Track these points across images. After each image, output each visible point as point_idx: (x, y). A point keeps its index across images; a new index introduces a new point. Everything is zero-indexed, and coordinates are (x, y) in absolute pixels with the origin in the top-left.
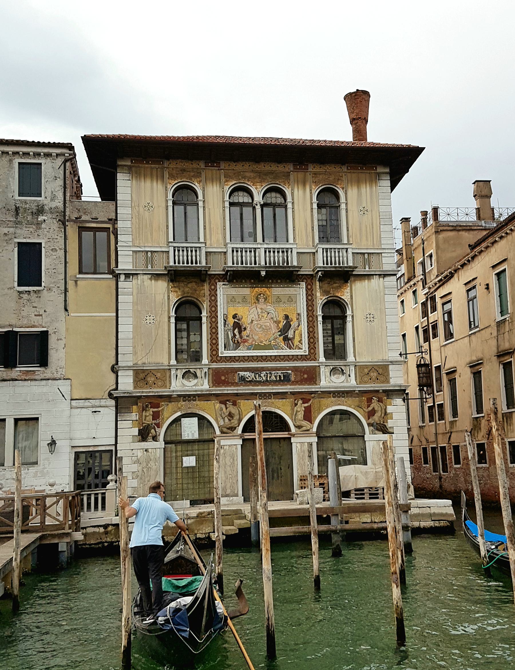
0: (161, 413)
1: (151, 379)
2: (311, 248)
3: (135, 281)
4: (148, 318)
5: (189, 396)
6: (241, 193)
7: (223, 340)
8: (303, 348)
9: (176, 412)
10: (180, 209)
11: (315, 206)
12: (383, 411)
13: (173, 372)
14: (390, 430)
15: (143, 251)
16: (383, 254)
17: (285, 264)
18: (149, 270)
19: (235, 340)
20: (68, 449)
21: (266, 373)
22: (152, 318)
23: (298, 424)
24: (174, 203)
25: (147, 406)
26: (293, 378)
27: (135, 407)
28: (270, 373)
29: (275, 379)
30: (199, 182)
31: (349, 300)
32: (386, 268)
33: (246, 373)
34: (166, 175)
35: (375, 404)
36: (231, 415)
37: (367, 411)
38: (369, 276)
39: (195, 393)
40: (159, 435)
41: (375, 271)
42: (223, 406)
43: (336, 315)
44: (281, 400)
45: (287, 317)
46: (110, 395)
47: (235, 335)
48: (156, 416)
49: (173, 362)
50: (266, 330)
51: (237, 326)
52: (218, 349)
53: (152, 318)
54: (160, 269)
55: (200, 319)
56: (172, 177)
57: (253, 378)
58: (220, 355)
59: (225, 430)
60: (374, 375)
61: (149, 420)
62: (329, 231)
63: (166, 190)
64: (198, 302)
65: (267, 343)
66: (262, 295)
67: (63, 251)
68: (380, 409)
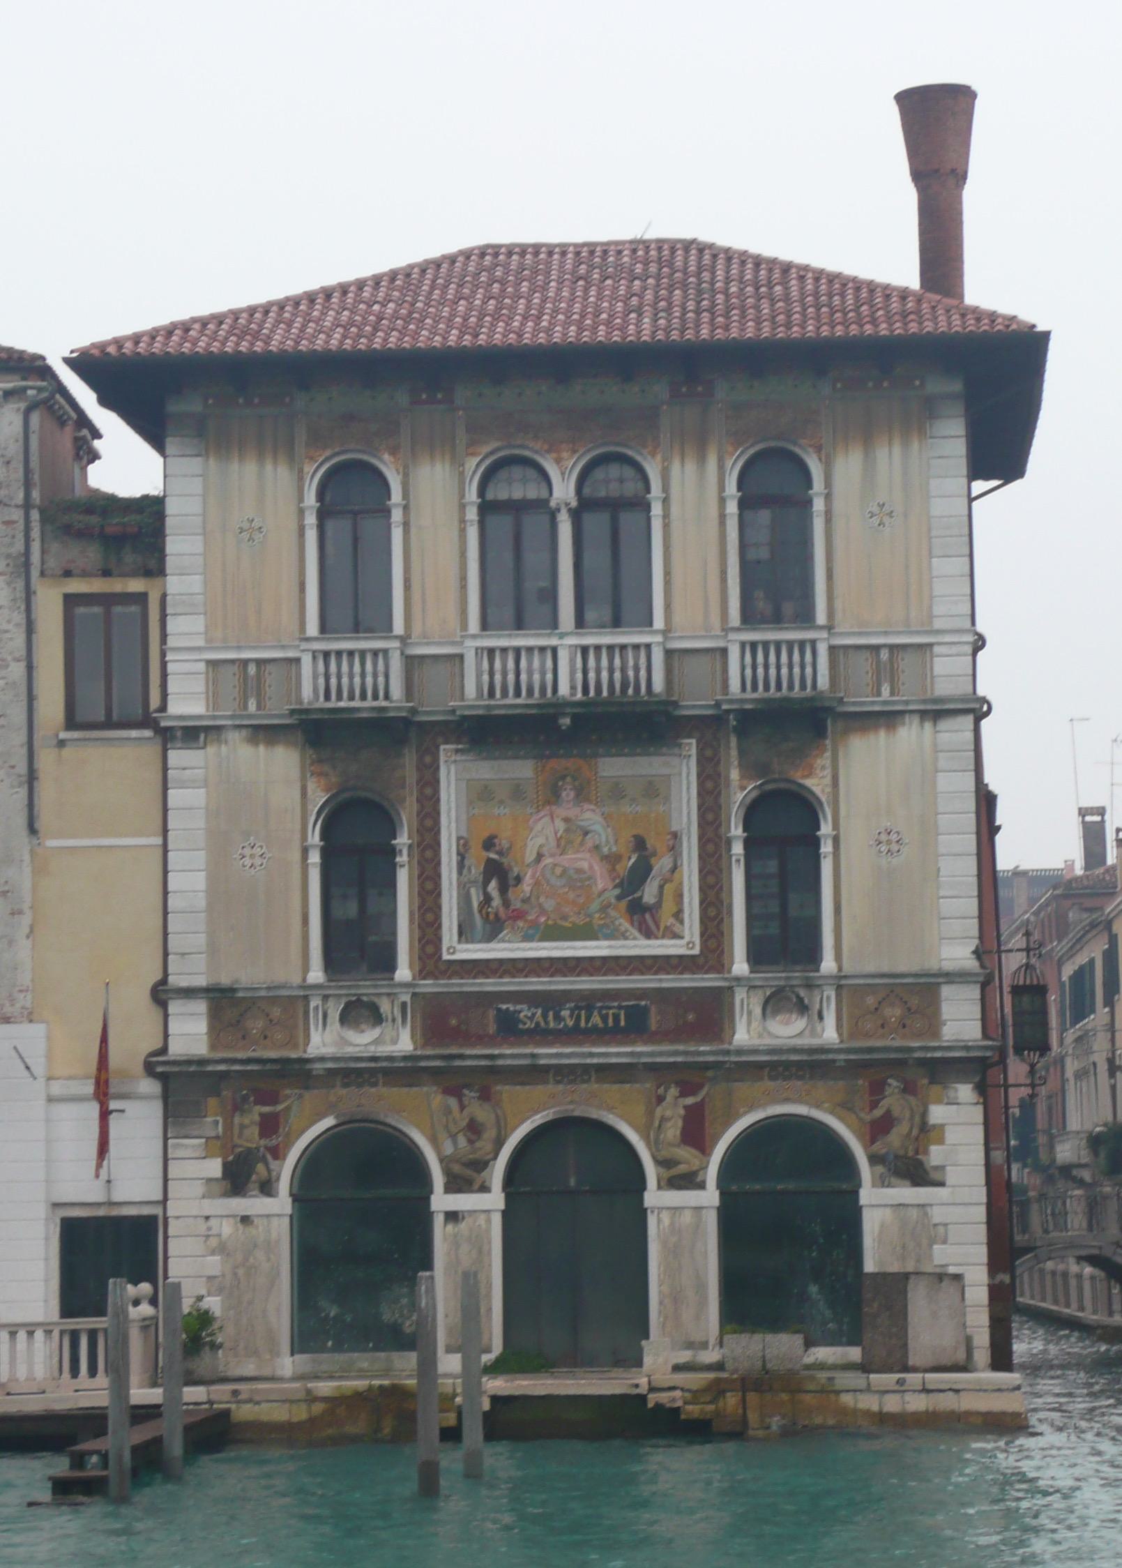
0: (282, 1120)
1: (256, 1025)
2: (717, 637)
3: (211, 750)
4: (247, 851)
5: (359, 1072)
6: (517, 471)
7: (455, 913)
8: (687, 933)
9: (320, 1116)
10: (340, 528)
11: (732, 508)
12: (917, 1119)
13: (312, 1005)
14: (935, 1176)
15: (233, 661)
16: (936, 649)
17: (630, 691)
18: (250, 716)
19: (488, 914)
20: (41, 1211)
21: (577, 1007)
22: (258, 851)
23: (665, 1154)
24: (323, 515)
25: (245, 1099)
26: (653, 1023)
27: (212, 1102)
28: (589, 1009)
29: (601, 1025)
30: (394, 451)
31: (828, 790)
32: (943, 688)
33: (519, 1007)
34: (301, 435)
35: (893, 1100)
36: (474, 1129)
37: (868, 1118)
38: (889, 718)
39: (373, 1065)
40: (278, 1179)
41: (907, 703)
42: (453, 1102)
43: (786, 835)
44: (616, 1087)
45: (640, 844)
46: (149, 1068)
47: (488, 899)
48: (269, 1126)
49: (316, 975)
50: (579, 881)
51: (497, 871)
52: (440, 940)
53: (258, 851)
54: (277, 710)
55: (393, 852)
56: (317, 439)
57: (538, 1024)
58: (446, 957)
59: (457, 1168)
60: (893, 1013)
61: (251, 1137)
62: (776, 581)
63: (301, 479)
64: (385, 804)
65: (580, 920)
66: (569, 779)
67: (23, 665)
68: (907, 1114)
